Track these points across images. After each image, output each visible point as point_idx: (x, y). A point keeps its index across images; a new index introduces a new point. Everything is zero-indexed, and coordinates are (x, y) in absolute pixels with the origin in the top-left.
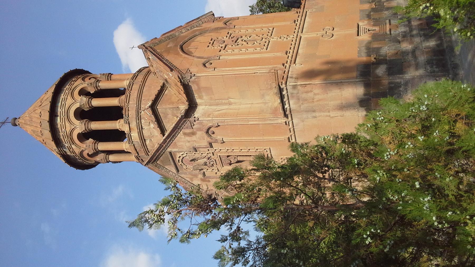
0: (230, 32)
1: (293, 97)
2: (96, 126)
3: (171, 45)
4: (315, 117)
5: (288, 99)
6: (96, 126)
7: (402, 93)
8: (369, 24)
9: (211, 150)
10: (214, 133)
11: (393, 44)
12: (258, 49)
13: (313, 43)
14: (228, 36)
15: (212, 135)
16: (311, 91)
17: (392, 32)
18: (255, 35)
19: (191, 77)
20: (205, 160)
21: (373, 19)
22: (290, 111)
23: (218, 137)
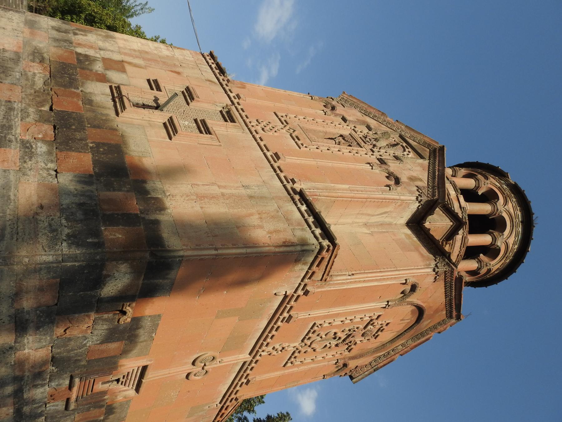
0: (347, 353)
1: (299, 224)
2: (484, 208)
4: (246, 187)
5: (306, 221)
6: (484, 208)
7: (64, 221)
8: (114, 394)
10: (387, 177)
11: (72, 354)
12: (326, 325)
13: (231, 344)
14: (353, 346)
15: (387, 175)
16: (270, 232)
17: (67, 382)
18: (317, 350)
19: (436, 266)
20: (379, 144)
22: (293, 199)
23: (377, 171)
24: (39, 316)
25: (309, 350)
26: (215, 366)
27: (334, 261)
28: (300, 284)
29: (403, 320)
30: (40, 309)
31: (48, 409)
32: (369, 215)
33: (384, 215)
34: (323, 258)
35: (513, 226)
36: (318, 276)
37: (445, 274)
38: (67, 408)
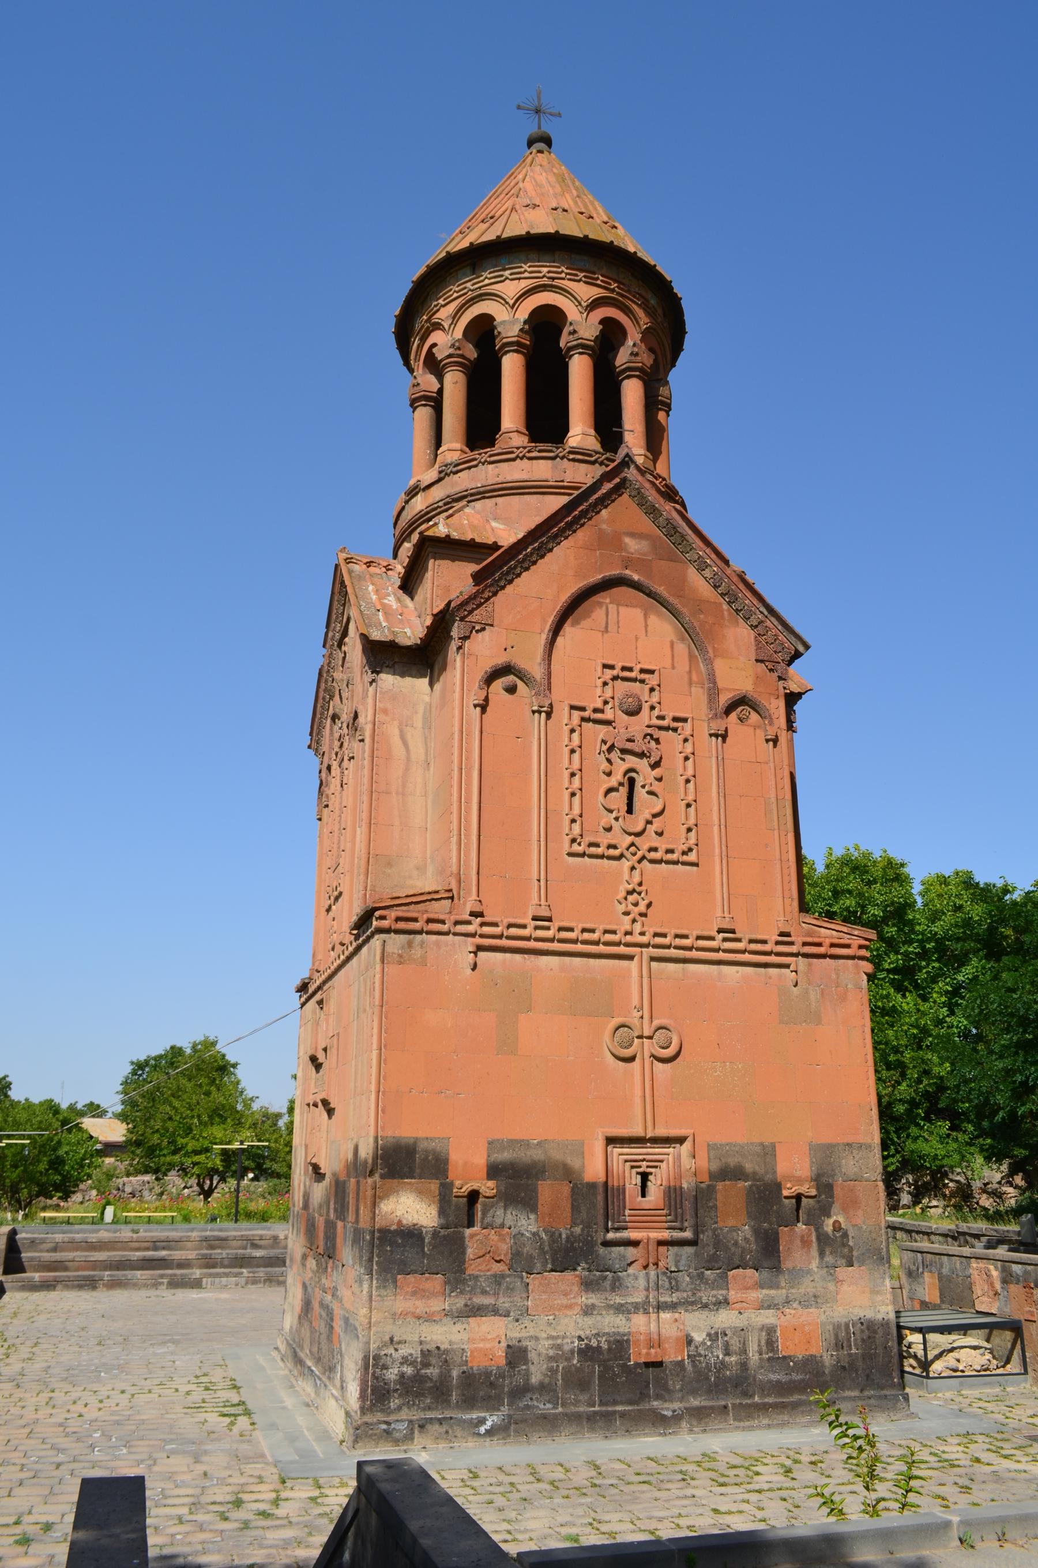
0: (688, 726)
2: (454, 387)
3: (633, 545)
9: (345, 731)
18: (657, 809)
21: (711, 1189)
24: (461, 1293)
25: (651, 829)
26: (646, 1016)
27: (407, 896)
28: (455, 934)
29: (607, 630)
30: (447, 1292)
31: (681, 1268)
32: (407, 769)
33: (409, 737)
34: (398, 919)
35: (481, 295)
36: (439, 909)
37: (473, 610)
38: (693, 1243)
